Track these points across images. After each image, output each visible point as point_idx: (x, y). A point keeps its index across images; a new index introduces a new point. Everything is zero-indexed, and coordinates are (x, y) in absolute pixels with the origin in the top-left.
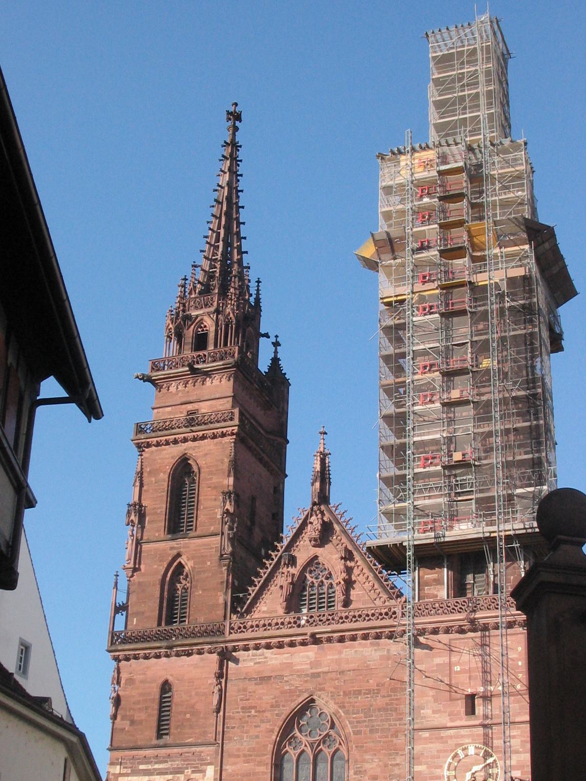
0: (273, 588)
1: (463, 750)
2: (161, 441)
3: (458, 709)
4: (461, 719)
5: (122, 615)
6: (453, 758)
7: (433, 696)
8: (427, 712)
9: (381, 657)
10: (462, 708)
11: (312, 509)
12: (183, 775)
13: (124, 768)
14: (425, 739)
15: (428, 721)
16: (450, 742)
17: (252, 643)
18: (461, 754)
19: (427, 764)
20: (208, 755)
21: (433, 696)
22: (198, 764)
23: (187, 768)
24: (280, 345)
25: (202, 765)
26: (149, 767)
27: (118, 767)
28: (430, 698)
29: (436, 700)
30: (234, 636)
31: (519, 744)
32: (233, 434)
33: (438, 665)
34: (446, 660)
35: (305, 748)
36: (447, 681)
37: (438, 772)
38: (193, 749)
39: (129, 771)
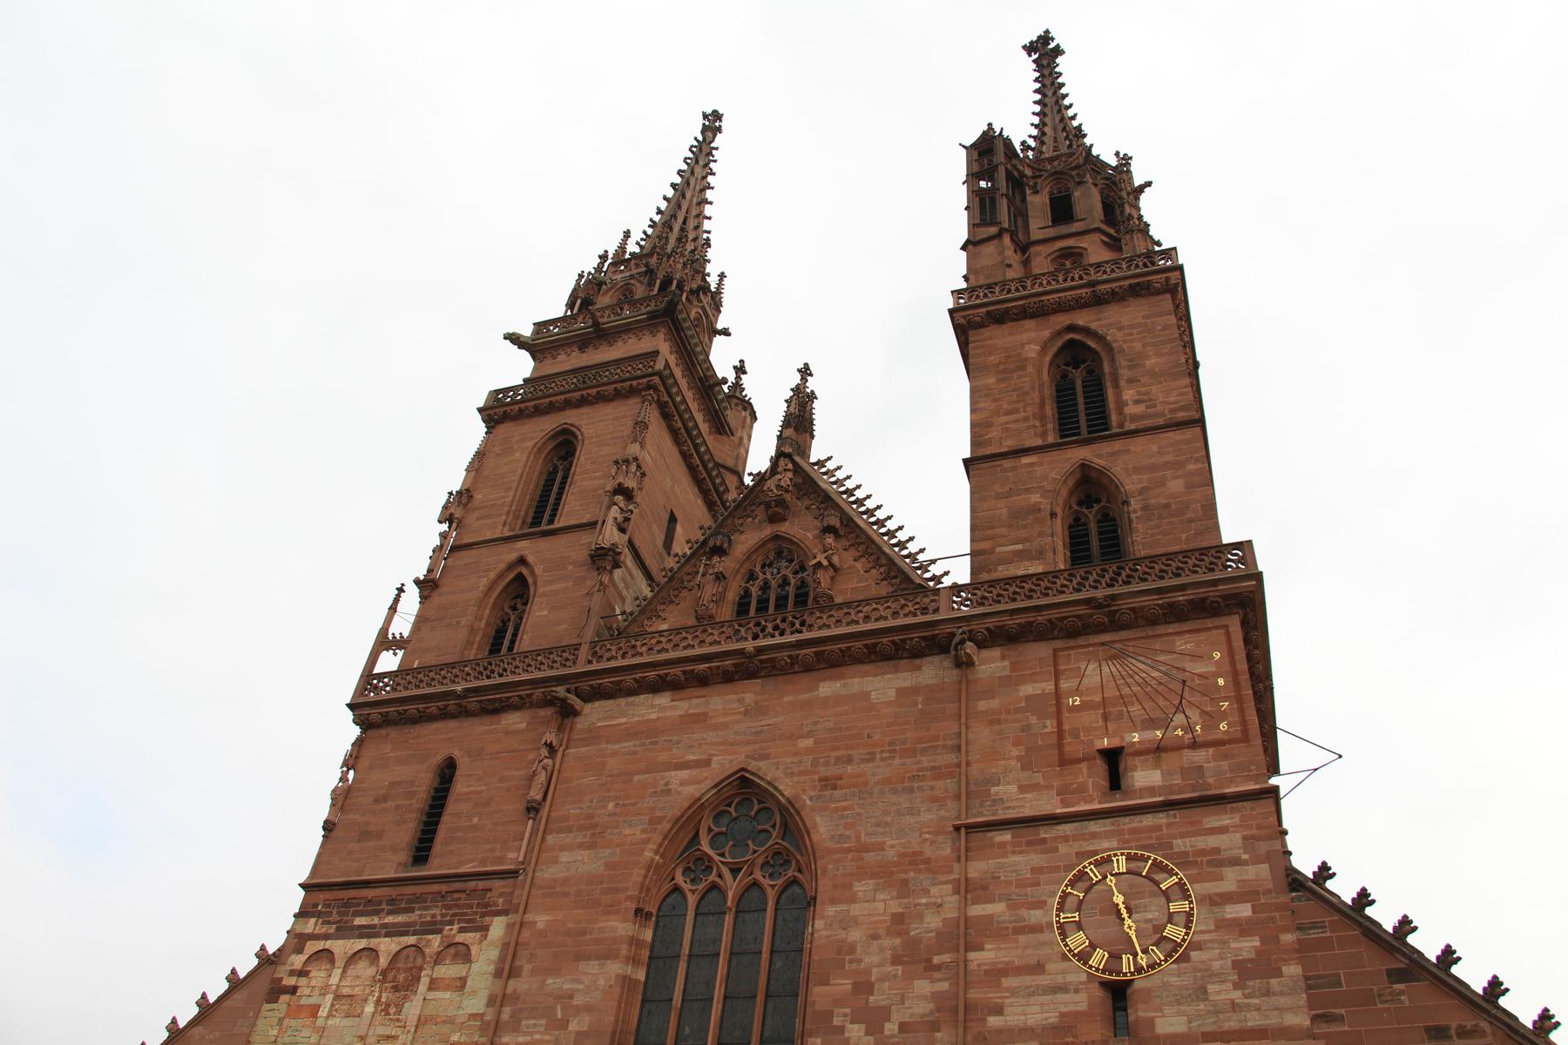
0: (686, 599)
1: (1097, 864)
2: (527, 408)
3: (1081, 780)
4: (1087, 801)
5: (395, 654)
6: (1072, 883)
7: (1018, 758)
8: (1007, 790)
9: (901, 692)
10: (1089, 776)
11: (775, 462)
12: (439, 936)
13: (328, 923)
14: (1003, 845)
15: (1008, 808)
16: (1063, 849)
17: (628, 679)
18: (1094, 874)
19: (1006, 898)
20: (500, 897)
21: (1018, 758)
22: (476, 913)
23: (451, 923)
24: (745, 373)
25: (483, 915)
26: (376, 921)
27: (313, 920)
28: (1013, 763)
29: (1026, 766)
30: (595, 666)
31: (1240, 841)
32: (648, 387)
33: (1028, 698)
34: (1049, 687)
35: (718, 880)
36: (1050, 726)
37: (1036, 916)
38: (472, 884)
39: (332, 929)
